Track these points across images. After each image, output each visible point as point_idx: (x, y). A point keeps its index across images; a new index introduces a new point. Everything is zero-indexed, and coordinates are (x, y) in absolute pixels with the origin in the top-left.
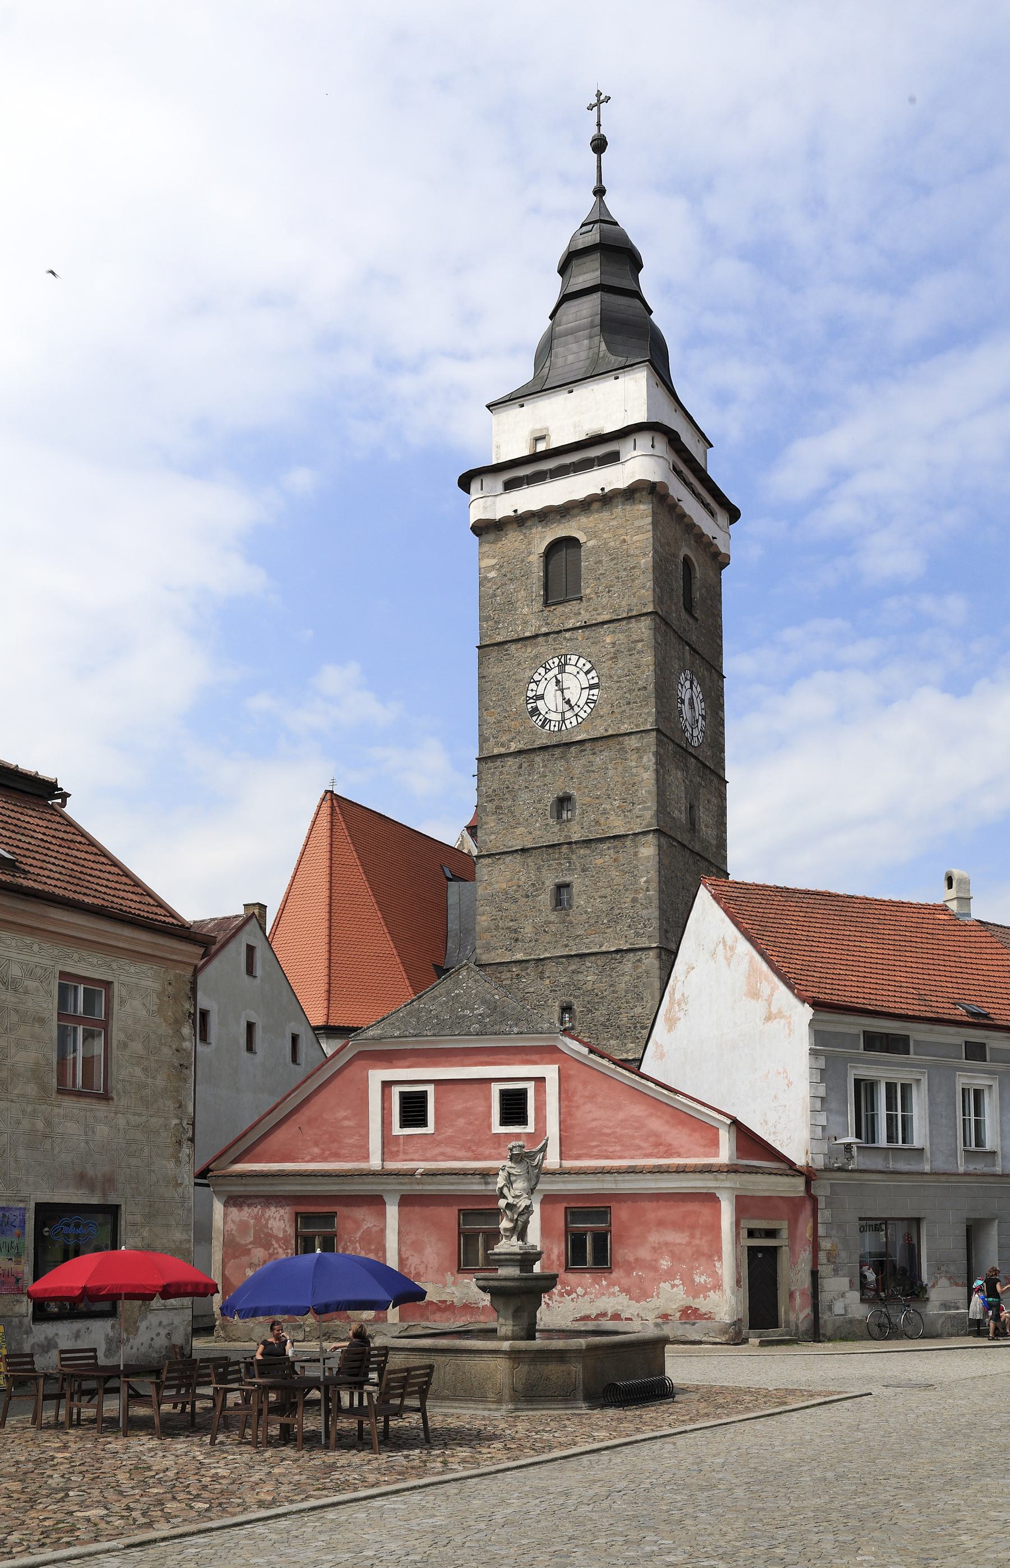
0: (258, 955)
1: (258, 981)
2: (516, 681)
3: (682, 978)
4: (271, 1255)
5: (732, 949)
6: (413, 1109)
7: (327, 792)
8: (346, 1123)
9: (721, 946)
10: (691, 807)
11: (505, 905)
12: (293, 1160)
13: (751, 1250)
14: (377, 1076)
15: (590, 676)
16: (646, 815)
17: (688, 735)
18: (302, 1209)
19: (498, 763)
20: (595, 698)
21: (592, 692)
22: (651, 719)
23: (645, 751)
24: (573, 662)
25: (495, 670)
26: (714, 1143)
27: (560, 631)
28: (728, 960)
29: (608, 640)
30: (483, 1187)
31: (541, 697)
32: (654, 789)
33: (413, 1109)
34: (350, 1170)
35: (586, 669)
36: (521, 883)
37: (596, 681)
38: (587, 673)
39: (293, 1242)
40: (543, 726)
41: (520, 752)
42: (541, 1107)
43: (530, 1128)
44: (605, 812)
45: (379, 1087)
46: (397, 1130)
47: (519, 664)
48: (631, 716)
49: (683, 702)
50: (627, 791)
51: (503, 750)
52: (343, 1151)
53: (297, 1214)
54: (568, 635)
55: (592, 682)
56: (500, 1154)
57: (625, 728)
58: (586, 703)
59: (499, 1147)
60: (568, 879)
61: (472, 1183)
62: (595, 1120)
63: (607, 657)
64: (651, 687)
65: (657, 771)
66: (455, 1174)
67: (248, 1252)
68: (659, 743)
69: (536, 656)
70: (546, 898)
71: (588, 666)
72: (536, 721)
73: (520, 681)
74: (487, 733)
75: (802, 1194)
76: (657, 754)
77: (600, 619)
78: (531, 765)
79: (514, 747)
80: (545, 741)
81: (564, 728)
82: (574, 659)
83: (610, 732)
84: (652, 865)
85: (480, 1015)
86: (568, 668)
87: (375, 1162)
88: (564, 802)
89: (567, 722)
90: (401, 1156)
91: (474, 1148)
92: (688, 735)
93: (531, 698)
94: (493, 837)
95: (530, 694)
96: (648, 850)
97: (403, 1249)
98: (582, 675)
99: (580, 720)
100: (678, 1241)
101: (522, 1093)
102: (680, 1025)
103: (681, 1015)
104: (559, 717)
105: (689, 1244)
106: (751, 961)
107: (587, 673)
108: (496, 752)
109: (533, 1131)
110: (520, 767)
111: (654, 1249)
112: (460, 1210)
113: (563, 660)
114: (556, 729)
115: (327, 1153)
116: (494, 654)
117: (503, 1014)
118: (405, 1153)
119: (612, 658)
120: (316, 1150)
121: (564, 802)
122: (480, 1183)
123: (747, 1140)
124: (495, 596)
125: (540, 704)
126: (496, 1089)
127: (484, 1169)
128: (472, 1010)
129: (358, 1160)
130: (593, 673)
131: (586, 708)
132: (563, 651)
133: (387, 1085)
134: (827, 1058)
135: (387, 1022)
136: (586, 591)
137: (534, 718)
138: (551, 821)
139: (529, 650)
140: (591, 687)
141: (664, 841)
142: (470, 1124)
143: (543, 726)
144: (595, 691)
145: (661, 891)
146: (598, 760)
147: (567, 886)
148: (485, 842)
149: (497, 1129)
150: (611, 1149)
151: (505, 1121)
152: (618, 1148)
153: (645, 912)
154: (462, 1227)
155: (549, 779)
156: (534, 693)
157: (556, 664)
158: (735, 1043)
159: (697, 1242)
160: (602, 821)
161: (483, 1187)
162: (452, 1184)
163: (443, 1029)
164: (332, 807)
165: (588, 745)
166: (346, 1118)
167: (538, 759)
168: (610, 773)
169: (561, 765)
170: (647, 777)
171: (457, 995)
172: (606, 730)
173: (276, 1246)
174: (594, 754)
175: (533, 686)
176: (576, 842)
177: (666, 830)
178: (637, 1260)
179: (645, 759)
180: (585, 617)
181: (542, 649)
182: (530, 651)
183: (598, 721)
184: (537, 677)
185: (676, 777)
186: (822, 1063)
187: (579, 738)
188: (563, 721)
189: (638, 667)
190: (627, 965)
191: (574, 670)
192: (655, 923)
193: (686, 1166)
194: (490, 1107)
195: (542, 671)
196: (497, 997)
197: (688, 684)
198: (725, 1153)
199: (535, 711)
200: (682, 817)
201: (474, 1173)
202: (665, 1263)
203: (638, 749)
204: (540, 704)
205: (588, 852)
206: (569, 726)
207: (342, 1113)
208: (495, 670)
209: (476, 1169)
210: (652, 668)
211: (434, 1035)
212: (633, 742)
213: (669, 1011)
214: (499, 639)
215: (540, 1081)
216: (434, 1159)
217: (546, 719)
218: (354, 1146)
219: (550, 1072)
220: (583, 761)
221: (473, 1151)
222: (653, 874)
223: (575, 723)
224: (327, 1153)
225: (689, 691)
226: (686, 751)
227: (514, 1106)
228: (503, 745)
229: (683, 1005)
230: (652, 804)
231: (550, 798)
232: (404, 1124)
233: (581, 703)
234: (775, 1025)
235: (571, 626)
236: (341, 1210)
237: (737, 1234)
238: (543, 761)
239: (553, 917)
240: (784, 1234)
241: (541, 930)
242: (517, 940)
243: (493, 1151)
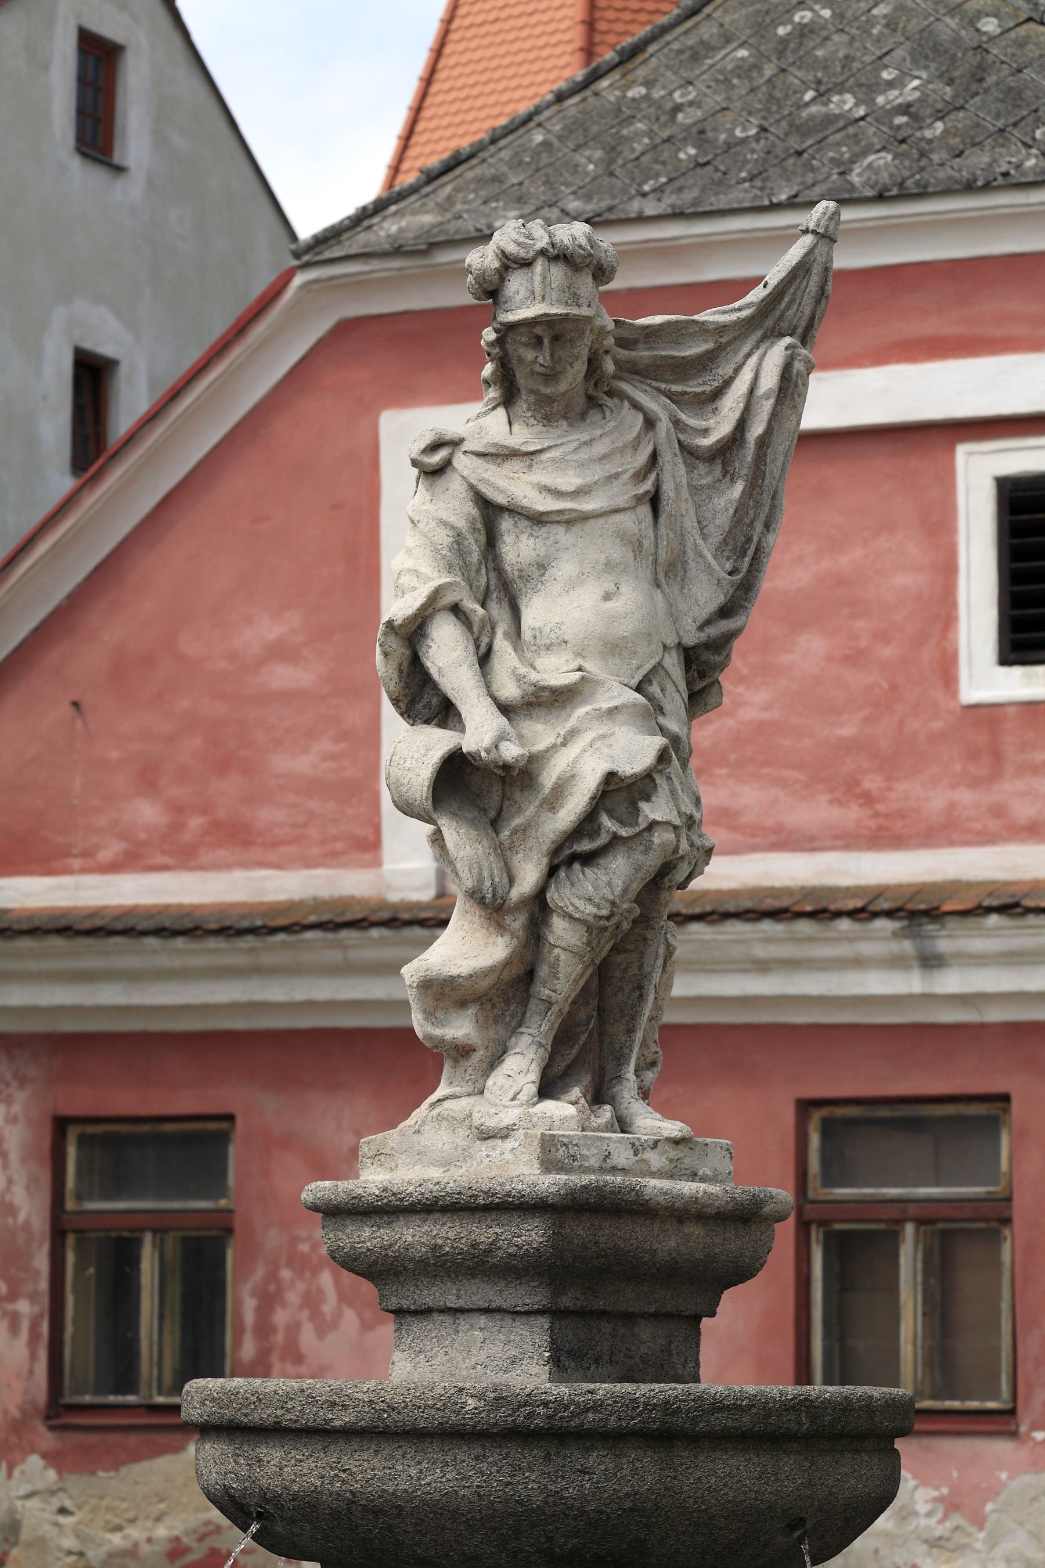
0: (136, 81)
1: (131, 190)
8: (283, 676)
12: (45, 861)
18: (81, 1100)
30: (910, 983)
34: (291, 906)
39: (42, 1262)
52: (266, 815)
53: (61, 1125)
56: (998, 811)
59: (996, 774)
61: (859, 963)
66: (775, 914)
85: (905, 109)
91: (872, 783)
112: (805, 1106)
115: (196, 823)
117: (1014, 96)
120: (147, 813)
122: (895, 963)
126: (978, 475)
127: (920, 890)
128: (868, 89)
129: (330, 858)
135: (468, 173)
142: (855, 658)
149: (987, 679)
154: (816, 1190)
161: (910, 983)
162: (763, 967)
163: (721, 184)
166: (281, 652)
171: (804, 31)
194: (947, 569)
196: (990, 25)
201: (865, 908)
207: (266, 629)
209: (880, 891)
211: (678, 215)
218: (313, 787)
221: (868, 799)
224: (196, 823)
236: (257, 1107)
243: (965, 796)
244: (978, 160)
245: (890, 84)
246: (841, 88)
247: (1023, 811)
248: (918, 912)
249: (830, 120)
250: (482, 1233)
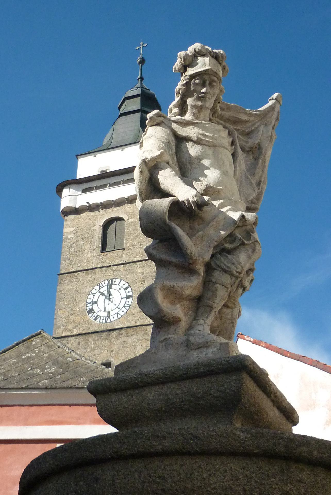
2: (80, 293)
15: (127, 291)
20: (130, 303)
21: (128, 300)
25: (68, 287)
27: (110, 266)
29: (139, 271)
31: (96, 303)
35: (125, 287)
37: (131, 294)
38: (126, 289)
40: (95, 319)
41: (79, 335)
47: (83, 284)
51: (68, 334)
54: (114, 268)
55: (128, 294)
58: (124, 306)
63: (139, 280)
71: (127, 285)
72: (91, 317)
73: (83, 293)
77: (135, 259)
78: (86, 342)
79: (75, 332)
80: (96, 329)
81: (109, 321)
83: (138, 323)
86: (113, 286)
89: (111, 317)
93: (89, 303)
95: (89, 301)
98: (122, 290)
99: (119, 316)
107: (126, 289)
110: (79, 344)
113: (110, 282)
114: (104, 321)
116: (68, 278)
119: (141, 281)
124: (71, 247)
125: (95, 307)
130: (129, 289)
131: (124, 309)
132: (111, 277)
136: (127, 245)
137: (90, 315)
139: (90, 276)
140: (128, 297)
143: (95, 319)
144: (130, 300)
146: (130, 340)
155: (96, 352)
156: (91, 300)
157: (106, 284)
165: (123, 331)
167: (91, 339)
169: (105, 343)
171: (28, 358)
172: (136, 322)
174: (127, 336)
175: (91, 296)
180: (126, 259)
181: (97, 276)
182: (90, 276)
184: (93, 291)
187: (118, 327)
188: (109, 316)
191: (118, 287)
195: (97, 288)
199: (91, 311)
204: (95, 307)
206: (112, 320)
217: (97, 316)
220: (120, 341)
223: (116, 318)
228: (69, 330)
233: (121, 306)
235: (117, 263)
238: (94, 340)
244: (68, 383)
245: (48, 368)
246: (37, 368)
249: (33, 374)
250: (196, 387)
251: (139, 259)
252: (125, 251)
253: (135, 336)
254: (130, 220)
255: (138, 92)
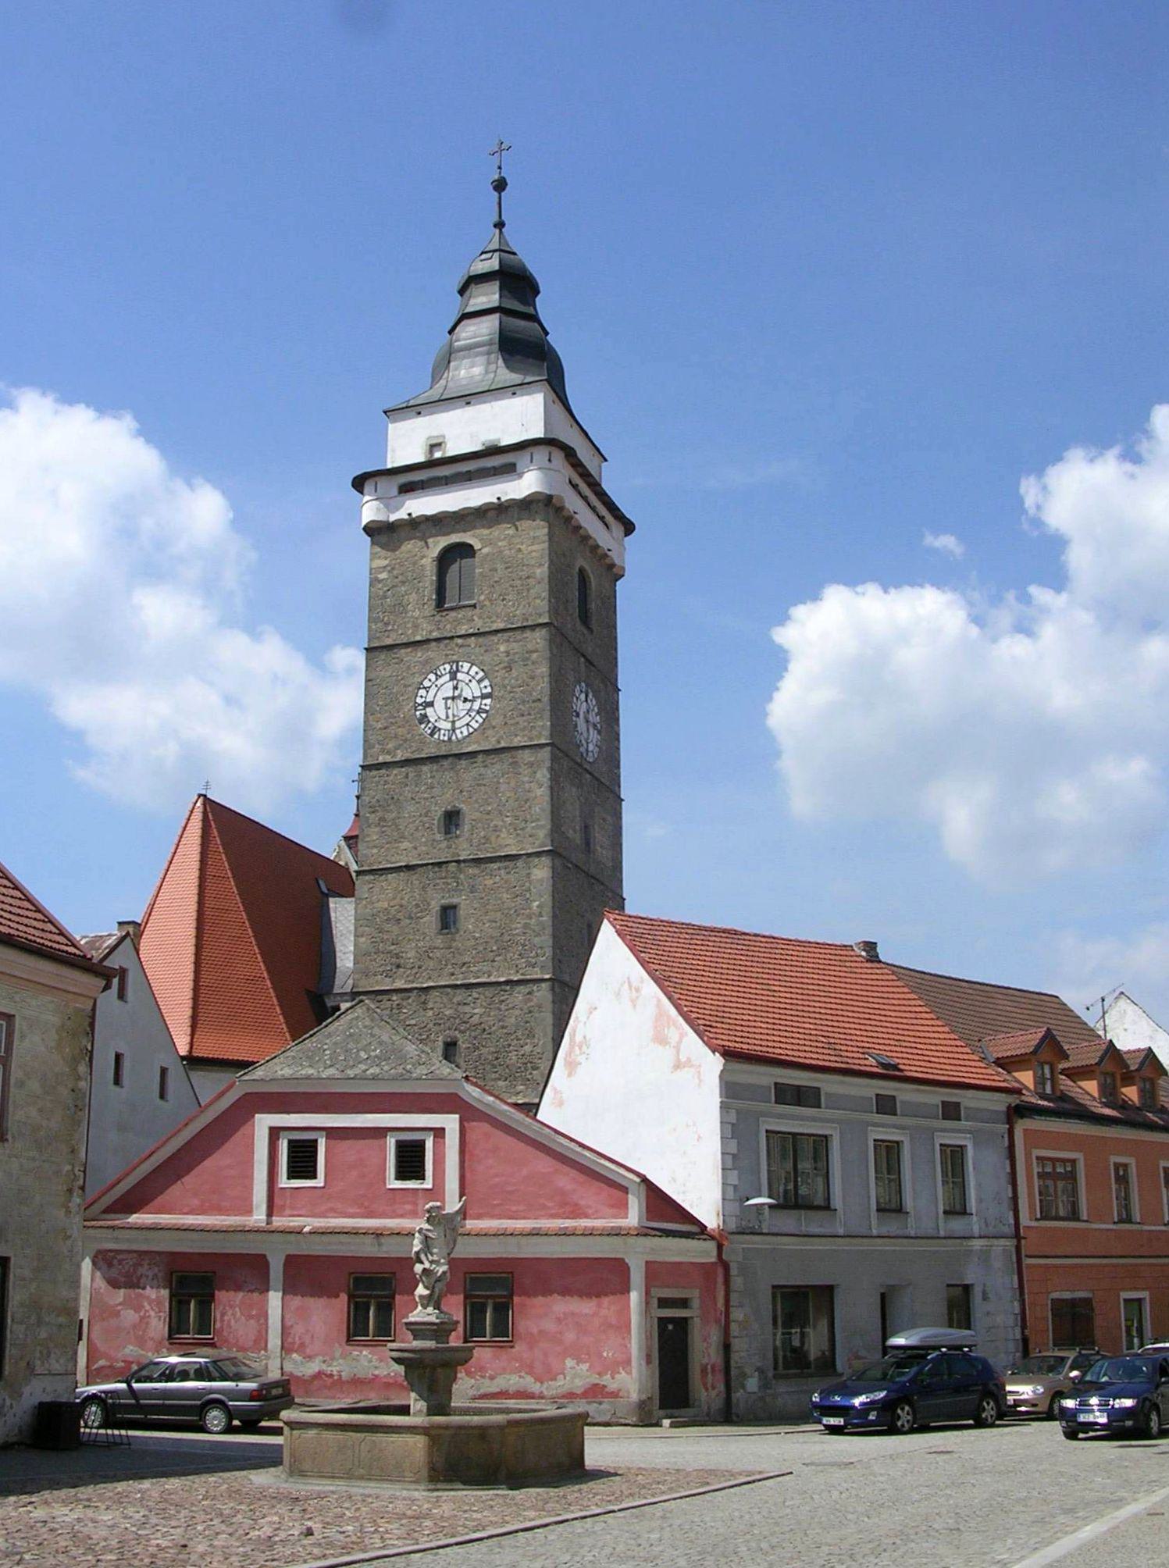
2: (405, 686)
3: (583, 1019)
4: (142, 1318)
5: (637, 990)
6: (302, 1160)
7: (200, 796)
9: (626, 986)
10: (586, 827)
11: (387, 927)
13: (663, 1322)
14: (264, 1122)
16: (540, 837)
17: (582, 749)
19: (383, 771)
22: (546, 733)
23: (539, 766)
24: (465, 669)
26: (623, 1206)
27: (452, 638)
28: (634, 1002)
29: (502, 648)
31: (431, 704)
32: (548, 808)
33: (302, 1160)
36: (404, 902)
37: (489, 690)
39: (167, 1304)
40: (432, 734)
42: (439, 1161)
43: (428, 1184)
44: (496, 829)
45: (267, 1131)
46: (284, 1182)
48: (524, 728)
49: (578, 715)
50: (518, 810)
51: (388, 759)
52: (224, 1204)
54: (460, 641)
57: (517, 741)
60: (455, 901)
62: (497, 1175)
64: (546, 699)
65: (551, 788)
67: (117, 1314)
68: (554, 758)
69: (426, 662)
70: (431, 921)
71: (481, 674)
74: (373, 739)
75: (713, 1260)
76: (552, 769)
77: (495, 627)
79: (400, 756)
80: (433, 751)
82: (466, 666)
83: (503, 744)
84: (546, 888)
86: (460, 676)
87: (259, 1217)
88: (452, 819)
90: (288, 1212)
92: (582, 749)
94: (375, 851)
95: (419, 700)
96: (541, 872)
97: (287, 1317)
100: (587, 1311)
101: (420, 1146)
102: (580, 1070)
103: (581, 1059)
104: (449, 726)
105: (595, 1314)
106: (659, 1005)
107: (479, 682)
108: (381, 759)
109: (430, 1186)
110: (407, 777)
111: (559, 1320)
118: (292, 1208)
120: (196, 1202)
121: (452, 819)
123: (660, 1204)
124: (385, 597)
125: (429, 711)
126: (391, 1142)
130: (486, 683)
133: (275, 1133)
134: (738, 1112)
138: (438, 837)
140: (484, 697)
141: (558, 862)
143: (432, 734)
144: (488, 701)
145: (554, 916)
147: (454, 907)
148: (366, 856)
150: (514, 1208)
151: (401, 1175)
152: (521, 1208)
153: (537, 940)
155: (436, 791)
158: (640, 1093)
159: (604, 1312)
160: (493, 839)
164: (205, 813)
168: (503, 787)
169: (449, 776)
170: (541, 793)
173: (148, 1307)
175: (422, 692)
176: (464, 861)
177: (561, 850)
178: (540, 1332)
179: (539, 775)
180: (479, 624)
182: (420, 654)
183: (490, 732)
184: (426, 683)
185: (571, 793)
186: (733, 1117)
187: (469, 749)
189: (533, 678)
190: (518, 995)
191: (467, 678)
192: (549, 952)
193: (593, 1228)
195: (432, 677)
197: (583, 697)
198: (633, 1215)
199: (424, 718)
200: (577, 837)
202: (570, 1336)
203: (531, 765)
205: (476, 871)
208: (384, 673)
210: (546, 679)
212: (526, 756)
213: (570, 1053)
214: (389, 642)
215: (439, 1133)
216: (323, 1215)
219: (450, 1122)
220: (474, 773)
222: (547, 898)
225: (583, 704)
226: (580, 765)
227: (410, 1160)
228: (388, 753)
229: (584, 1048)
230: (545, 822)
231: (438, 812)
232: (293, 1174)
234: (686, 1074)
235: (463, 632)
237: (647, 1303)
239: (439, 941)
240: (696, 1303)
241: (427, 953)
242: (398, 966)
247: (400, 1212)
248: (378, 1234)
251: (501, 626)
252: (477, 611)
253: (497, 766)
254: (485, 551)
255: (493, 264)
